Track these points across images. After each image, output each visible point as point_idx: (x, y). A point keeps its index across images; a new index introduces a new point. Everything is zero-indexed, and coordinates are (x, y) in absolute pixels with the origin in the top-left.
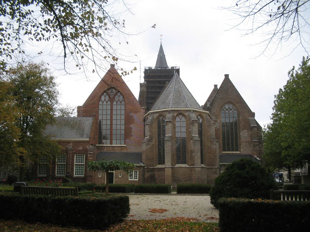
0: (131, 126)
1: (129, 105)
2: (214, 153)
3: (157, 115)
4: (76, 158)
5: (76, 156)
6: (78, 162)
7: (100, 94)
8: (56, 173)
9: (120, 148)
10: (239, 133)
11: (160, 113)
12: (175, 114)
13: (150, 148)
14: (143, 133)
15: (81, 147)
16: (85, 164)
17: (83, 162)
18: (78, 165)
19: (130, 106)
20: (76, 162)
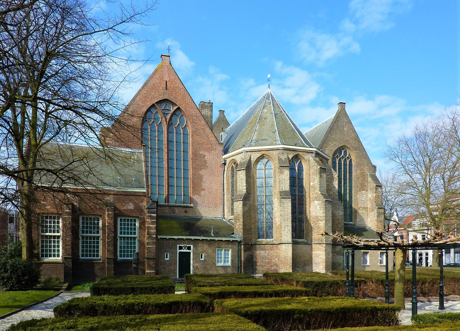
0: (201, 172)
1: (198, 135)
2: (339, 223)
3: (258, 155)
4: (121, 224)
5: (121, 220)
6: (124, 233)
7: (145, 109)
8: (80, 253)
9: (183, 210)
10: (355, 196)
11: (263, 152)
12: (291, 157)
13: (247, 210)
14: (223, 185)
15: (131, 204)
16: (139, 237)
17: (135, 233)
18: (124, 238)
19: (200, 138)
20: (121, 233)
